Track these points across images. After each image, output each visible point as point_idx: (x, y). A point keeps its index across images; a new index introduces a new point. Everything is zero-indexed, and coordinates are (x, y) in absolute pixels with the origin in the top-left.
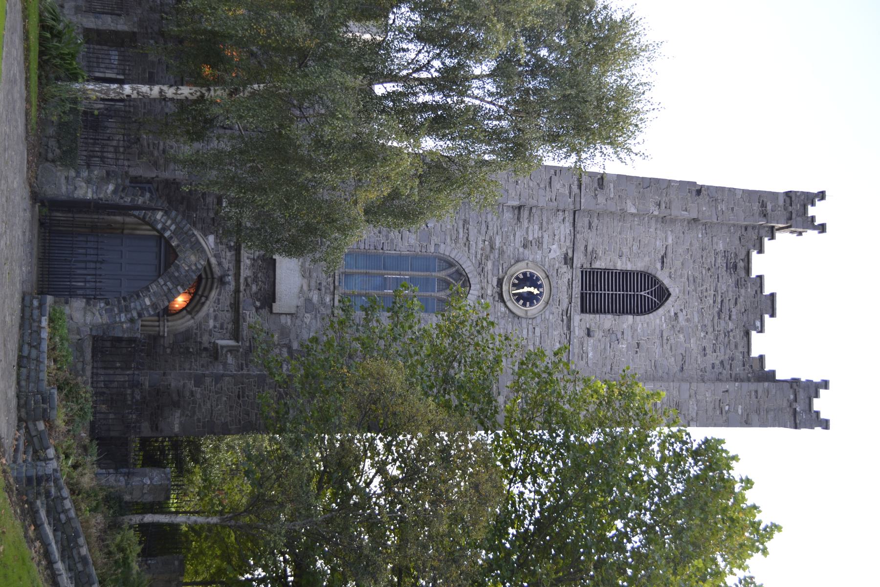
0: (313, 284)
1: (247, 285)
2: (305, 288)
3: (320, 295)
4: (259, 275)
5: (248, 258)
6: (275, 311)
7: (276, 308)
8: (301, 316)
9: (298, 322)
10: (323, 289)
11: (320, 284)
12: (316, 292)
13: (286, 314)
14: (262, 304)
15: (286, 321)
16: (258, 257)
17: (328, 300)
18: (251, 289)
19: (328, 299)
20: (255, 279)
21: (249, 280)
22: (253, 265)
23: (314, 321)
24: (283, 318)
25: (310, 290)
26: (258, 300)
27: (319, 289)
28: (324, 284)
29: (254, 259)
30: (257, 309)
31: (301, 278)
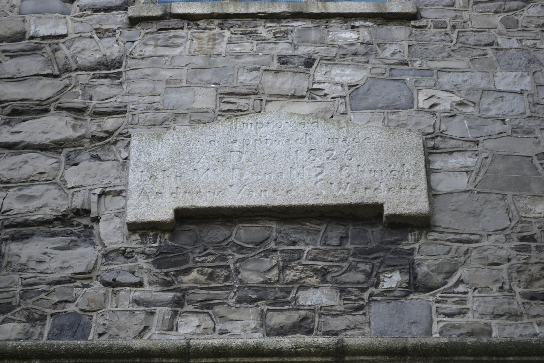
0: (287, 82)
1: (302, 326)
2: (305, 107)
3: (330, 60)
4: (254, 279)
5: (172, 327)
6: (420, 205)
7: (405, 198)
8: (427, 123)
9: (456, 128)
10: (304, 50)
11: (283, 60)
12: (319, 73)
13: (429, 172)
14: (392, 267)
15: (455, 173)
16: (166, 285)
17: (350, 36)
18: (326, 311)
19: (346, 35)
20: (277, 295)
21: (278, 319)
22: (206, 306)
23: (445, 78)
24: (443, 183)
25: (313, 93)
26: (373, 278)
27: (309, 63)
28: (283, 48)
29: (178, 303)
30: (415, 285)
31: (260, 118)
